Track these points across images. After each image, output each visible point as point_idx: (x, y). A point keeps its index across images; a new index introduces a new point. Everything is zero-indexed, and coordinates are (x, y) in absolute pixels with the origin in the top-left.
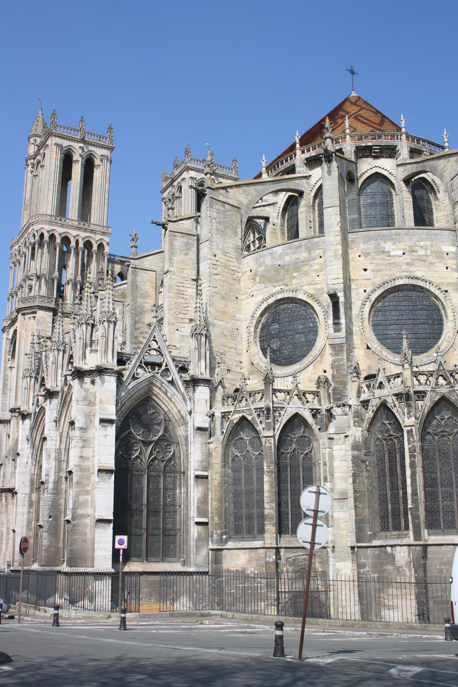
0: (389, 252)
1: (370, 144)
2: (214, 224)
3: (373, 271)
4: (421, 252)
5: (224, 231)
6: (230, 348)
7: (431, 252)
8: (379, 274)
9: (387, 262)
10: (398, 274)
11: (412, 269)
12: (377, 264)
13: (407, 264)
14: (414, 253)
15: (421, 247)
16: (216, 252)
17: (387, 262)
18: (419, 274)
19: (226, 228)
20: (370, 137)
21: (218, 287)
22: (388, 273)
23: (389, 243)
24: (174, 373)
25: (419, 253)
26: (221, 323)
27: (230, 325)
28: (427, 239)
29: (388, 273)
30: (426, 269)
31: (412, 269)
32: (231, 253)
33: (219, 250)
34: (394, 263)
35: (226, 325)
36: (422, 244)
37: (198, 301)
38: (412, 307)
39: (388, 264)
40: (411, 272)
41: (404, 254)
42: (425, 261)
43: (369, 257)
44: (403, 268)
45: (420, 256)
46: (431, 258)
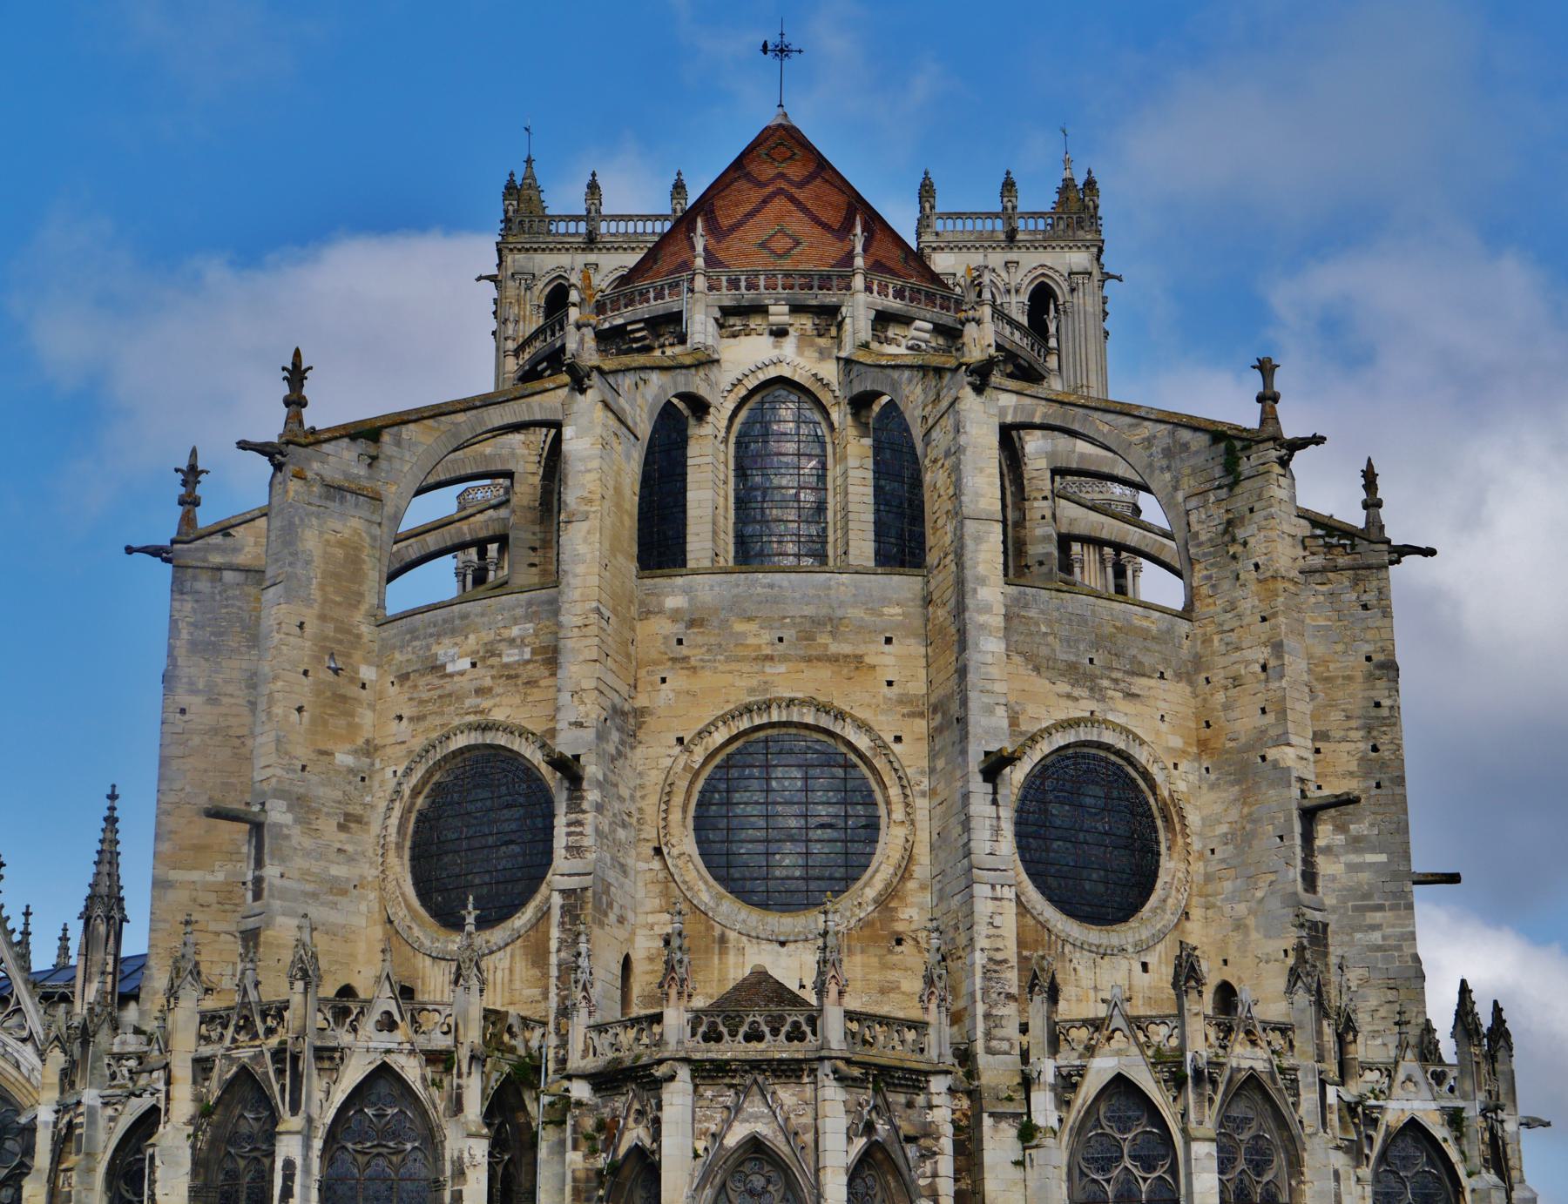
0: (443, 666)
1: (620, 321)
2: (185, 635)
3: (411, 719)
4: (510, 656)
5: (214, 644)
6: (218, 934)
7: (533, 652)
8: (423, 725)
9: (439, 692)
10: (456, 722)
11: (486, 704)
12: (422, 702)
13: (480, 692)
14: (493, 661)
15: (511, 641)
16: (184, 699)
17: (439, 692)
18: (498, 715)
19: (221, 634)
20: (622, 302)
21: (188, 789)
22: (438, 721)
23: (446, 641)
24: (34, 1019)
25: (505, 659)
26: (195, 875)
27: (220, 876)
28: (529, 618)
29: (438, 721)
30: (517, 700)
31: (486, 704)
32: (238, 693)
33: (194, 692)
34: (450, 695)
35: (209, 878)
36: (515, 631)
37: (109, 835)
38: (489, 803)
39: (440, 697)
40: (482, 712)
41: (474, 665)
42: (517, 676)
43: (409, 683)
44: (468, 703)
45: (506, 666)
46: (530, 667)
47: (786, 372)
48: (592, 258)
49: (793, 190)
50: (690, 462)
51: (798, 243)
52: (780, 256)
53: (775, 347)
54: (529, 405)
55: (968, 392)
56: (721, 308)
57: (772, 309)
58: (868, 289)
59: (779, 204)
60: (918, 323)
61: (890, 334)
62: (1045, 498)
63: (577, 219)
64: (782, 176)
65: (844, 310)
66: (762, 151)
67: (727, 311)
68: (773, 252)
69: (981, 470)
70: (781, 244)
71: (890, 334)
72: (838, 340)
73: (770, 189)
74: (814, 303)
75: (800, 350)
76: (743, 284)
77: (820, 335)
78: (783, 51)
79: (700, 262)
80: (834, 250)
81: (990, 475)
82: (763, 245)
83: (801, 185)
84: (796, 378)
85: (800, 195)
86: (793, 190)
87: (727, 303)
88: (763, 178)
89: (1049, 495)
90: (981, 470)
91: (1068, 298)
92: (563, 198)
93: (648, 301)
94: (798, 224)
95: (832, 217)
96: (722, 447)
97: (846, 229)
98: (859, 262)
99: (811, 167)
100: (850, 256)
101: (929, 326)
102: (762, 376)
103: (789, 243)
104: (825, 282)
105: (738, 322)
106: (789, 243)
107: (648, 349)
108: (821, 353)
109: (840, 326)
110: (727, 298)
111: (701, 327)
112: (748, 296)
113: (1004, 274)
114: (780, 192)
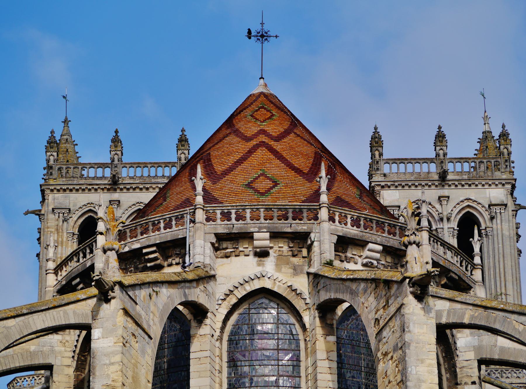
1: (137, 246)
20: (139, 231)
47: (268, 284)
48: (116, 196)
49: (272, 143)
50: (192, 356)
51: (276, 184)
52: (262, 194)
53: (259, 265)
54: (65, 313)
55: (411, 301)
56: (216, 235)
57: (256, 235)
58: (332, 219)
59: (261, 152)
60: (371, 246)
61: (349, 255)
62: (474, 383)
63: (103, 166)
64: (263, 132)
65: (312, 235)
66: (248, 112)
67: (220, 238)
68: (256, 191)
69: (422, 361)
70: (263, 185)
71: (349, 255)
72: (309, 258)
73: (254, 142)
74: (289, 230)
75: (278, 267)
76: (233, 216)
77: (294, 256)
78: (263, 36)
79: (199, 199)
80: (304, 188)
81: (430, 365)
82: (249, 185)
83: (278, 139)
84: (276, 289)
85: (278, 146)
86: (272, 143)
87: (221, 230)
88: (249, 134)
89: (477, 380)
90: (422, 361)
91: (489, 224)
92: (92, 151)
93: (159, 229)
94: (276, 169)
95: (304, 164)
96: (218, 344)
97: (314, 171)
98: (324, 198)
99: (286, 125)
100: (317, 194)
101: (380, 248)
102: (249, 288)
103: (268, 184)
104: (297, 215)
105: (230, 246)
106: (269, 184)
107: (159, 268)
108: (295, 269)
109: (309, 248)
110: (221, 227)
111: (200, 250)
112: (237, 226)
113: (438, 206)
114: (262, 144)
